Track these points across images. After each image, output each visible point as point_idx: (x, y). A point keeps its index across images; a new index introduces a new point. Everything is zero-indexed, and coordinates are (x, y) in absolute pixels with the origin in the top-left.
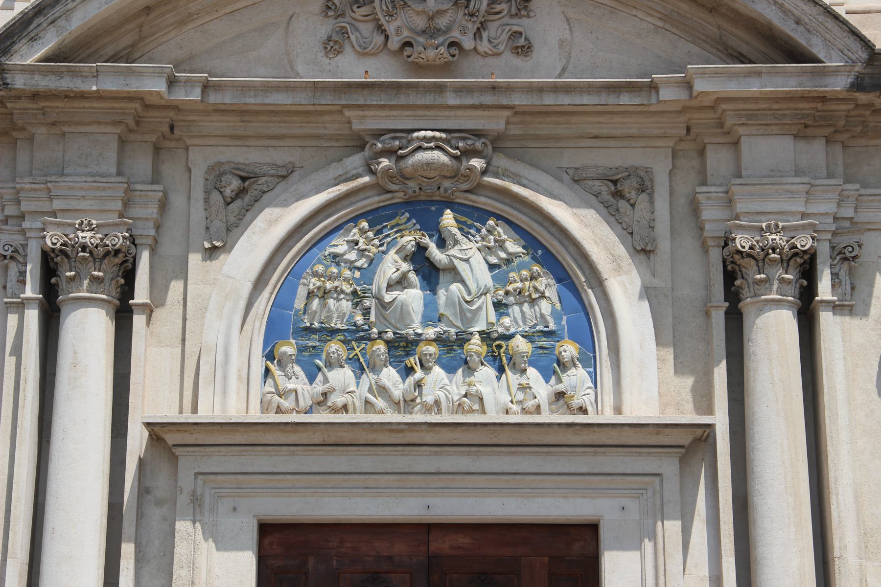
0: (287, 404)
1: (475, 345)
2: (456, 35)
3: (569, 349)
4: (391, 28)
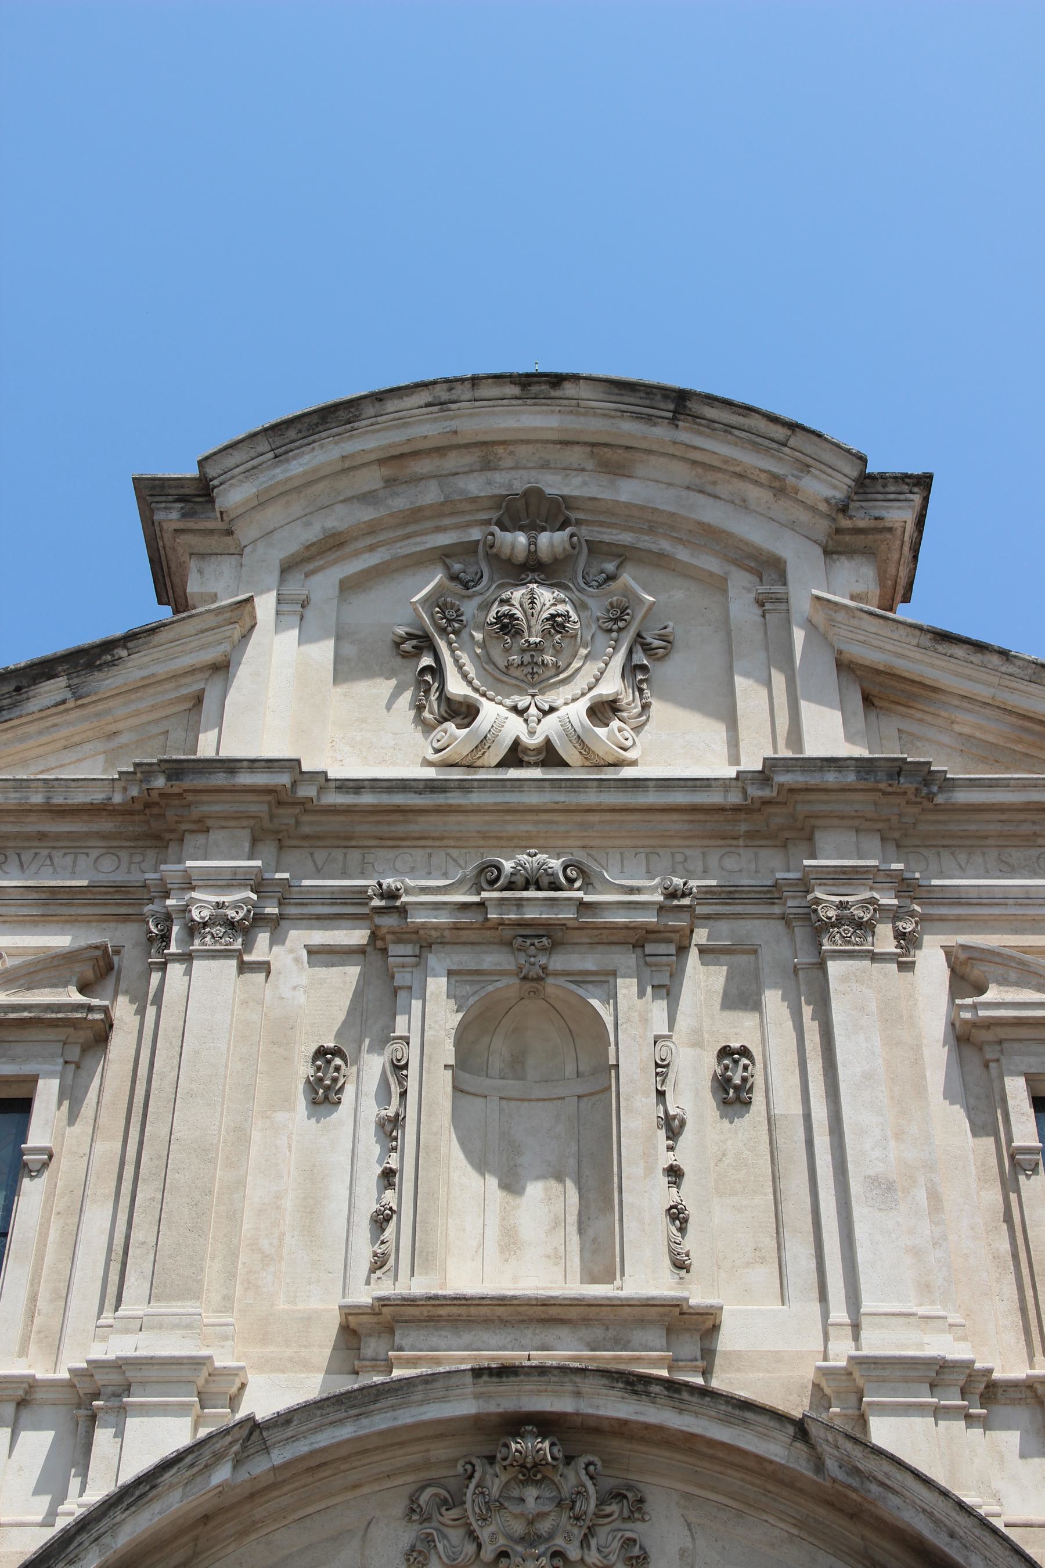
2: (559, 1542)
4: (484, 1535)
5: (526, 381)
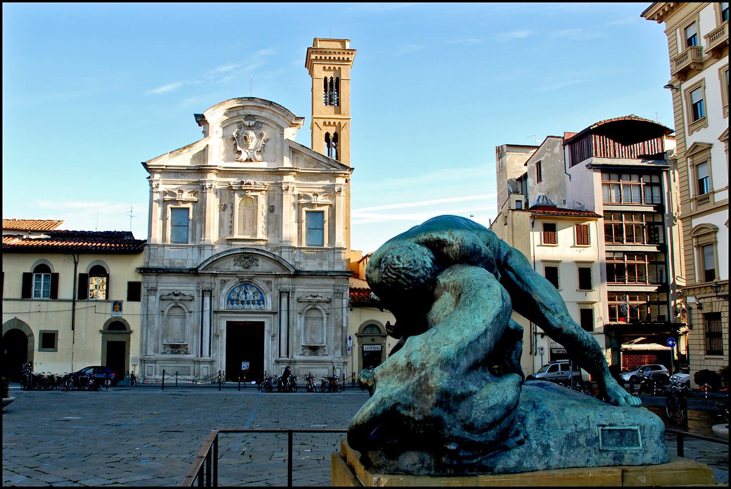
0: (229, 308)
1: (251, 302)
3: (261, 302)
5: (249, 98)
